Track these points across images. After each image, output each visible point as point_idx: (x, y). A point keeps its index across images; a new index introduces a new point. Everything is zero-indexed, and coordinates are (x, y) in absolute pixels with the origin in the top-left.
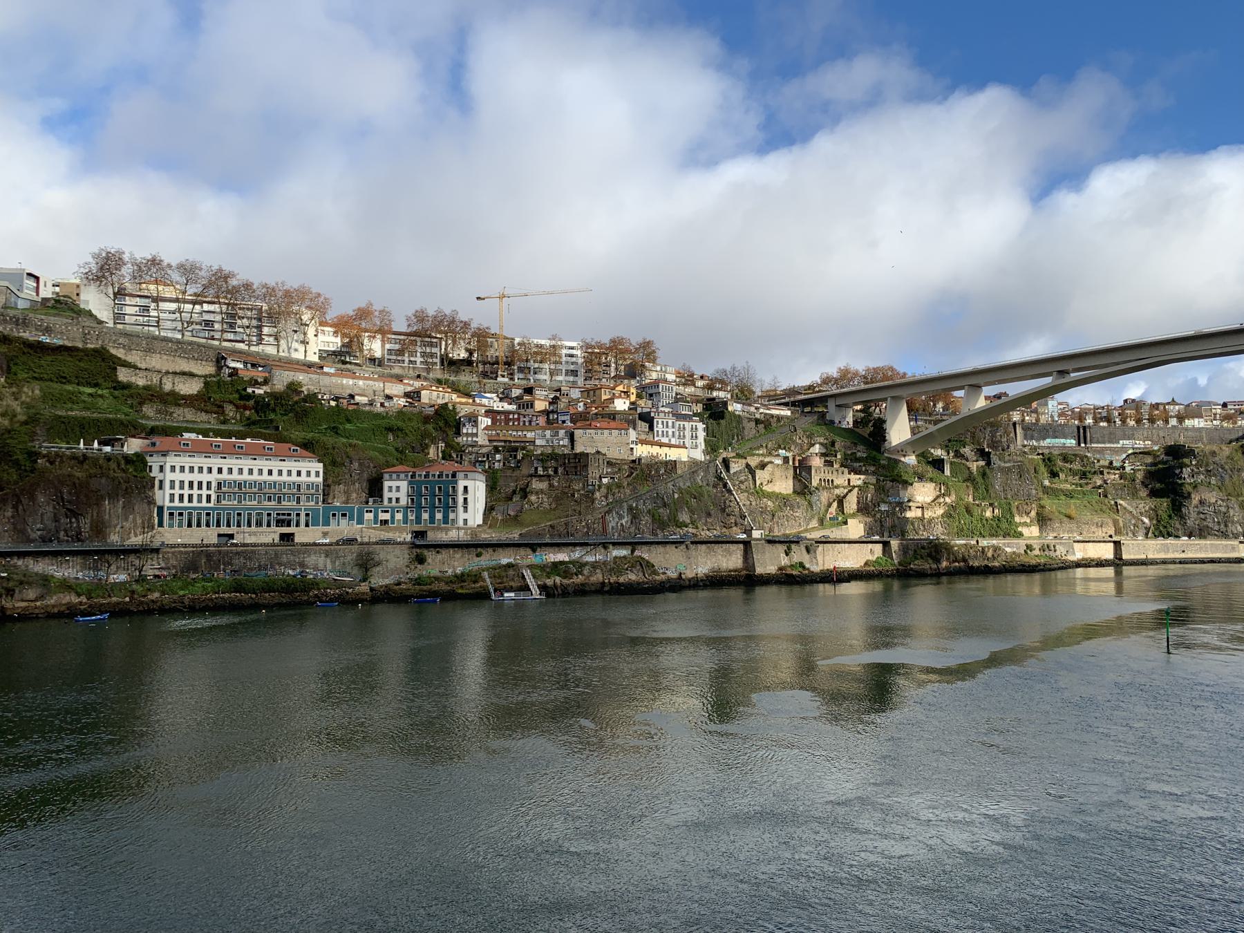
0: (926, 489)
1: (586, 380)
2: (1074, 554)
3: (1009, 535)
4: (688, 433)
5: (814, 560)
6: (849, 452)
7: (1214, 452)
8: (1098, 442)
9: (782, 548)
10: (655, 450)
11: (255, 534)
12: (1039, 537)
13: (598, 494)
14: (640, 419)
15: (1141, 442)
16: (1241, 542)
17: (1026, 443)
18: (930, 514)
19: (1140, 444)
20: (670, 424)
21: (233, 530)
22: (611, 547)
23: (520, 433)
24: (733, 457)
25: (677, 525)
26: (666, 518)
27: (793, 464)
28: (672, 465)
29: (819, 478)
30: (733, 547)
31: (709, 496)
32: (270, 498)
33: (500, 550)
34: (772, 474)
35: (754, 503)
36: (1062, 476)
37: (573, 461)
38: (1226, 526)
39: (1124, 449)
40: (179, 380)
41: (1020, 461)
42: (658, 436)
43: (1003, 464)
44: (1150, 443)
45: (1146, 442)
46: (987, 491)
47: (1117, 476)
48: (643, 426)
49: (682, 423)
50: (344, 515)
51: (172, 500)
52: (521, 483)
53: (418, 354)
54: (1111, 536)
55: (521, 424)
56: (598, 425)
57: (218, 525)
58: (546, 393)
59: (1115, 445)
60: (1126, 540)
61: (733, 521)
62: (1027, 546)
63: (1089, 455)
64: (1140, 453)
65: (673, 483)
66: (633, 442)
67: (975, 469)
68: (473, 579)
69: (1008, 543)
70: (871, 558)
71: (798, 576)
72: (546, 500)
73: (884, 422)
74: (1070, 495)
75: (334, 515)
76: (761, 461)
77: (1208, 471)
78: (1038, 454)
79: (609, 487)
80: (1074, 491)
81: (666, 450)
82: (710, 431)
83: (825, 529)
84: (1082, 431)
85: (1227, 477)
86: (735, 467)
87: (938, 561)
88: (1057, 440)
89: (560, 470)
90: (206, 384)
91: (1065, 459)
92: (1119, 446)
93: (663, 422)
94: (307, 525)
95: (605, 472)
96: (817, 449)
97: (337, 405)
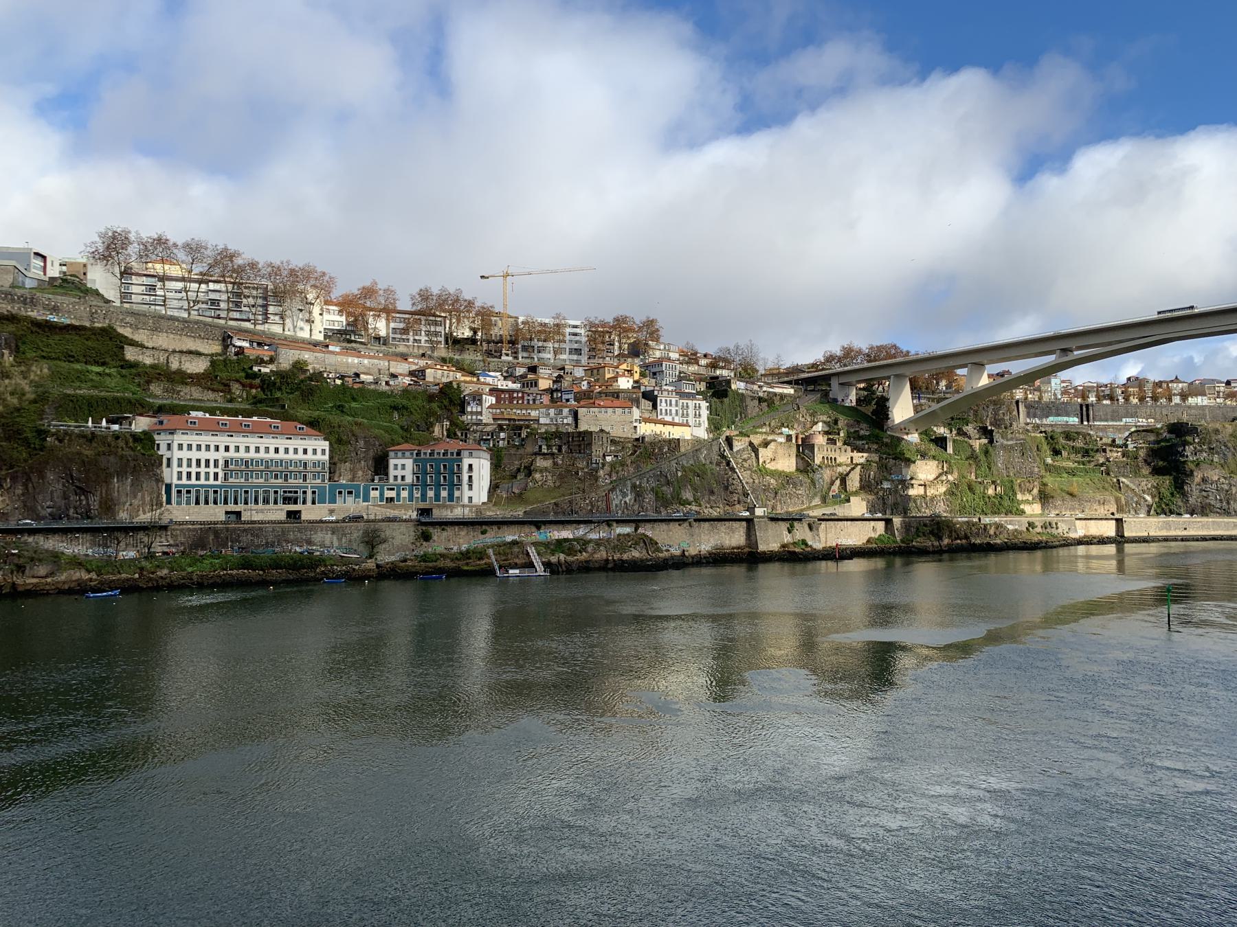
0: (929, 467)
1: (589, 358)
2: (1076, 531)
3: (1011, 512)
4: (691, 411)
5: (817, 538)
6: (852, 430)
8: (1101, 420)
9: (784, 526)
10: (658, 428)
11: (262, 511)
12: (1041, 515)
13: (601, 472)
14: (643, 397)
15: (1144, 420)
19: (1143, 422)
20: (673, 403)
21: (240, 507)
22: (615, 524)
23: (524, 412)
24: (737, 435)
27: (796, 441)
28: (675, 444)
30: (736, 525)
31: (712, 474)
35: (757, 481)
37: (577, 439)
39: (1126, 427)
40: (186, 359)
41: (1022, 439)
42: (661, 414)
43: (1005, 442)
44: (1153, 420)
45: (1149, 420)
46: (990, 469)
47: (1120, 454)
48: (646, 404)
49: (685, 401)
50: (350, 493)
51: (180, 478)
52: (526, 461)
53: (423, 333)
54: (1113, 514)
55: (525, 402)
56: (602, 403)
57: (226, 502)
59: (1118, 423)
60: (1128, 517)
63: (1092, 433)
64: (1144, 431)
66: (636, 420)
69: (1010, 521)
70: (873, 535)
72: (550, 478)
73: (888, 400)
74: (1072, 473)
75: (340, 493)
76: (764, 439)
77: (1211, 449)
78: (1041, 432)
79: (612, 465)
81: (669, 428)
82: (714, 410)
83: (827, 506)
84: (1084, 409)
85: (1229, 455)
86: (739, 445)
87: (940, 538)
88: (1060, 418)
89: (564, 448)
90: (213, 363)
91: (1068, 436)
93: (666, 400)
94: (314, 503)
97: (343, 384)
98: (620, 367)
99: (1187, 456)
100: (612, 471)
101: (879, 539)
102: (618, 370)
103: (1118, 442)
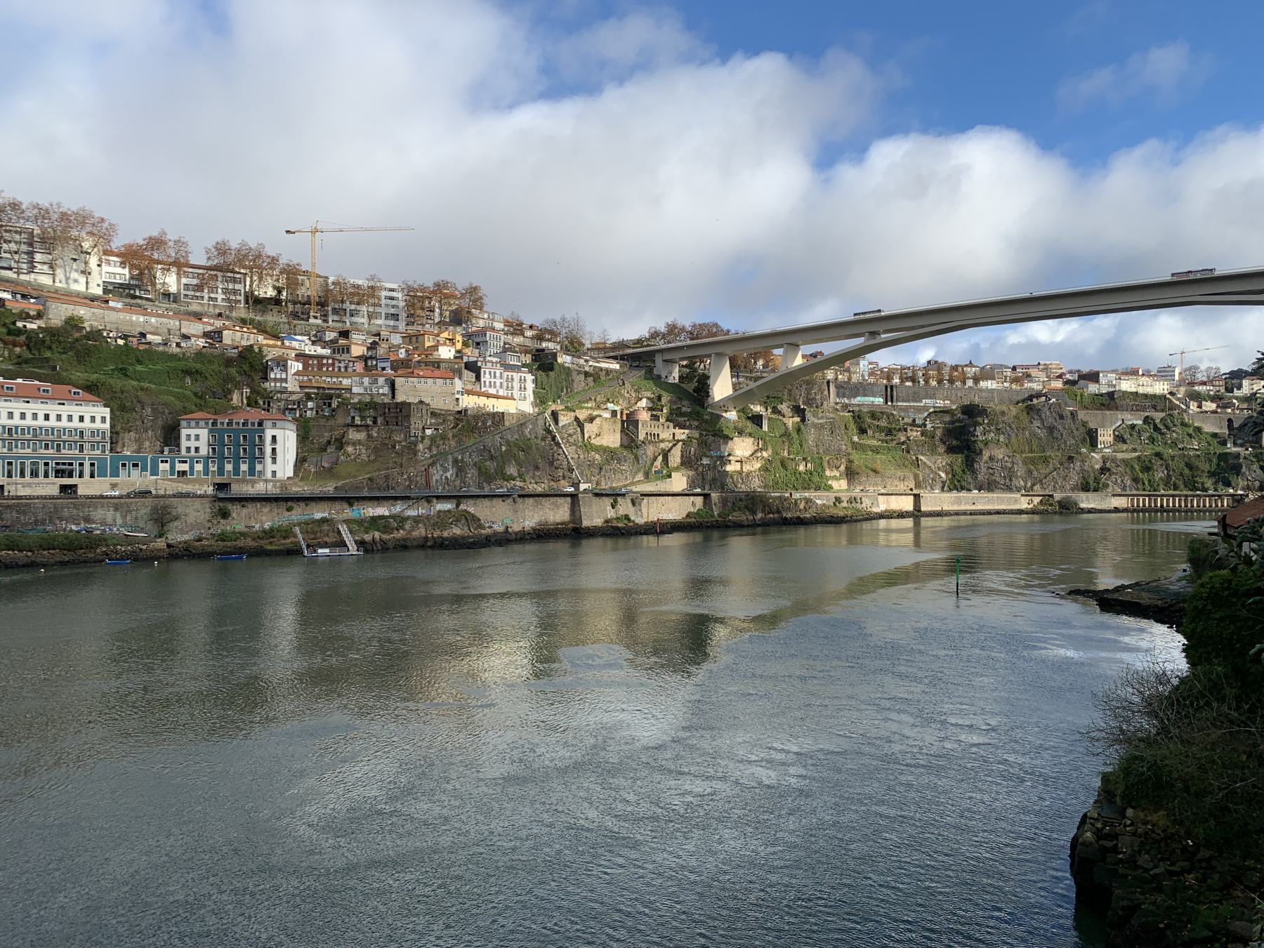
1: (407, 324)
2: (878, 506)
4: (516, 384)
5: (639, 513)
6: (675, 407)
7: (1004, 412)
8: (903, 401)
9: (607, 502)
10: (482, 401)
11: (29, 485)
12: (847, 490)
13: (421, 446)
14: (466, 368)
16: (1022, 495)
17: (838, 401)
18: (748, 468)
19: (940, 403)
22: (435, 500)
23: (335, 380)
24: (562, 410)
26: (492, 471)
28: (499, 418)
30: (560, 500)
32: (47, 447)
33: (313, 504)
35: (582, 457)
36: (870, 432)
37: (394, 410)
39: (925, 408)
42: (485, 386)
43: (816, 421)
44: (949, 402)
49: (510, 374)
50: (135, 465)
52: (337, 433)
53: (220, 291)
54: (911, 490)
55: (336, 369)
56: (421, 373)
58: (363, 338)
59: (918, 404)
62: (836, 498)
63: (895, 413)
64: (940, 412)
65: (500, 435)
66: (458, 392)
67: (791, 425)
71: (623, 528)
72: (364, 451)
73: (708, 377)
74: (876, 451)
75: (124, 465)
76: (590, 414)
77: (997, 429)
78: (849, 411)
79: (432, 438)
81: (492, 401)
84: (889, 390)
85: (1013, 436)
86: (564, 420)
87: (754, 513)
88: (867, 399)
89: (379, 420)
91: (873, 415)
92: (922, 405)
93: (490, 372)
94: (92, 476)
95: (428, 423)
96: (643, 403)
97: (126, 344)
98: (441, 335)
100: (431, 445)
101: (698, 513)
102: (438, 338)
103: (918, 422)
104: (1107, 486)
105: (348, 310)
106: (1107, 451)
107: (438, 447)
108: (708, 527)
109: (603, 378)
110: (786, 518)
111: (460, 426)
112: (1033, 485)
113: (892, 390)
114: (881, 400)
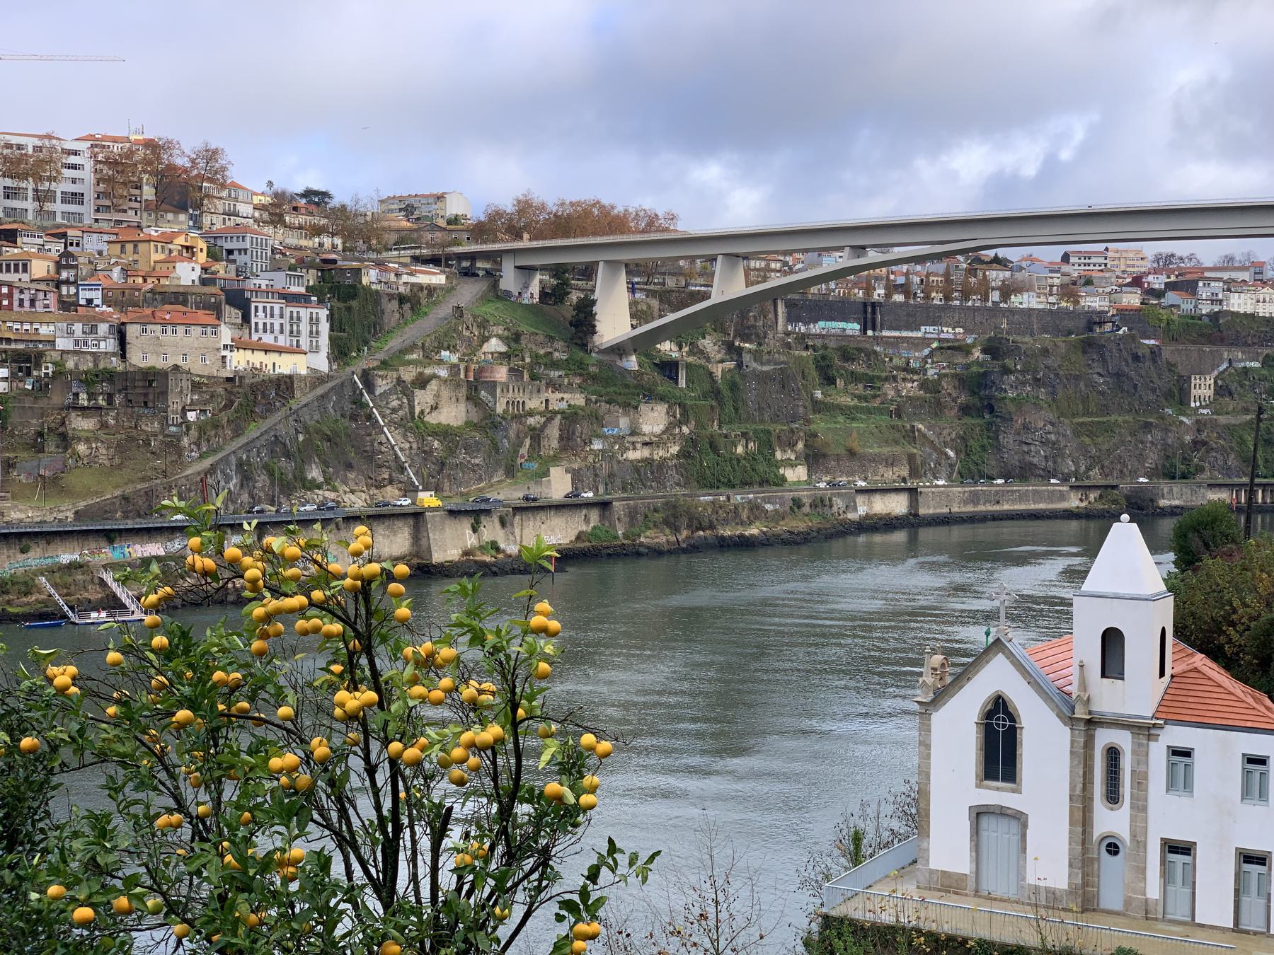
0: (656, 414)
1: (98, 210)
2: (855, 509)
3: (768, 482)
4: (304, 327)
5: (511, 538)
6: (542, 352)
8: (890, 328)
9: (465, 525)
10: (258, 358)
12: (808, 483)
13: (185, 439)
14: (228, 303)
15: (950, 330)
17: (790, 328)
18: (660, 454)
19: (948, 333)
20: (277, 311)
22: (229, 531)
23: (27, 326)
24: (378, 368)
25: (304, 487)
26: (290, 476)
27: (466, 377)
28: (285, 385)
29: (506, 400)
30: (399, 523)
31: (348, 436)
33: (58, 541)
34: (437, 396)
36: (840, 383)
37: (140, 384)
38: (1055, 462)
39: (925, 342)
41: (782, 363)
42: (257, 331)
43: (760, 368)
44: (961, 330)
45: (957, 330)
47: (916, 384)
48: (232, 314)
49: (295, 310)
52: (53, 419)
54: (904, 480)
55: (16, 303)
56: (168, 317)
58: (40, 241)
59: (911, 334)
60: (925, 487)
61: (386, 476)
62: (793, 500)
63: (878, 349)
64: (949, 348)
66: (225, 347)
67: (720, 374)
68: (23, 589)
69: (769, 497)
70: (584, 528)
71: (494, 565)
72: (103, 451)
73: (594, 302)
74: (849, 413)
76: (421, 374)
77: (1037, 380)
78: (807, 348)
79: (202, 429)
80: (856, 408)
81: (274, 357)
82: (336, 323)
83: (516, 483)
84: (869, 310)
85: (1060, 389)
86: (382, 386)
87: (676, 530)
89: (118, 399)
91: (846, 356)
92: (920, 335)
95: (189, 401)
96: (494, 345)
98: (176, 241)
99: (1005, 391)
100: (199, 438)
101: (593, 534)
102: (170, 246)
103: (912, 364)
104: (1202, 470)
105: (30, 199)
106: (1205, 411)
107: (209, 441)
108: (609, 555)
109: (424, 302)
110: (723, 538)
111: (236, 404)
112: (1088, 469)
113: (874, 312)
114: (857, 326)
